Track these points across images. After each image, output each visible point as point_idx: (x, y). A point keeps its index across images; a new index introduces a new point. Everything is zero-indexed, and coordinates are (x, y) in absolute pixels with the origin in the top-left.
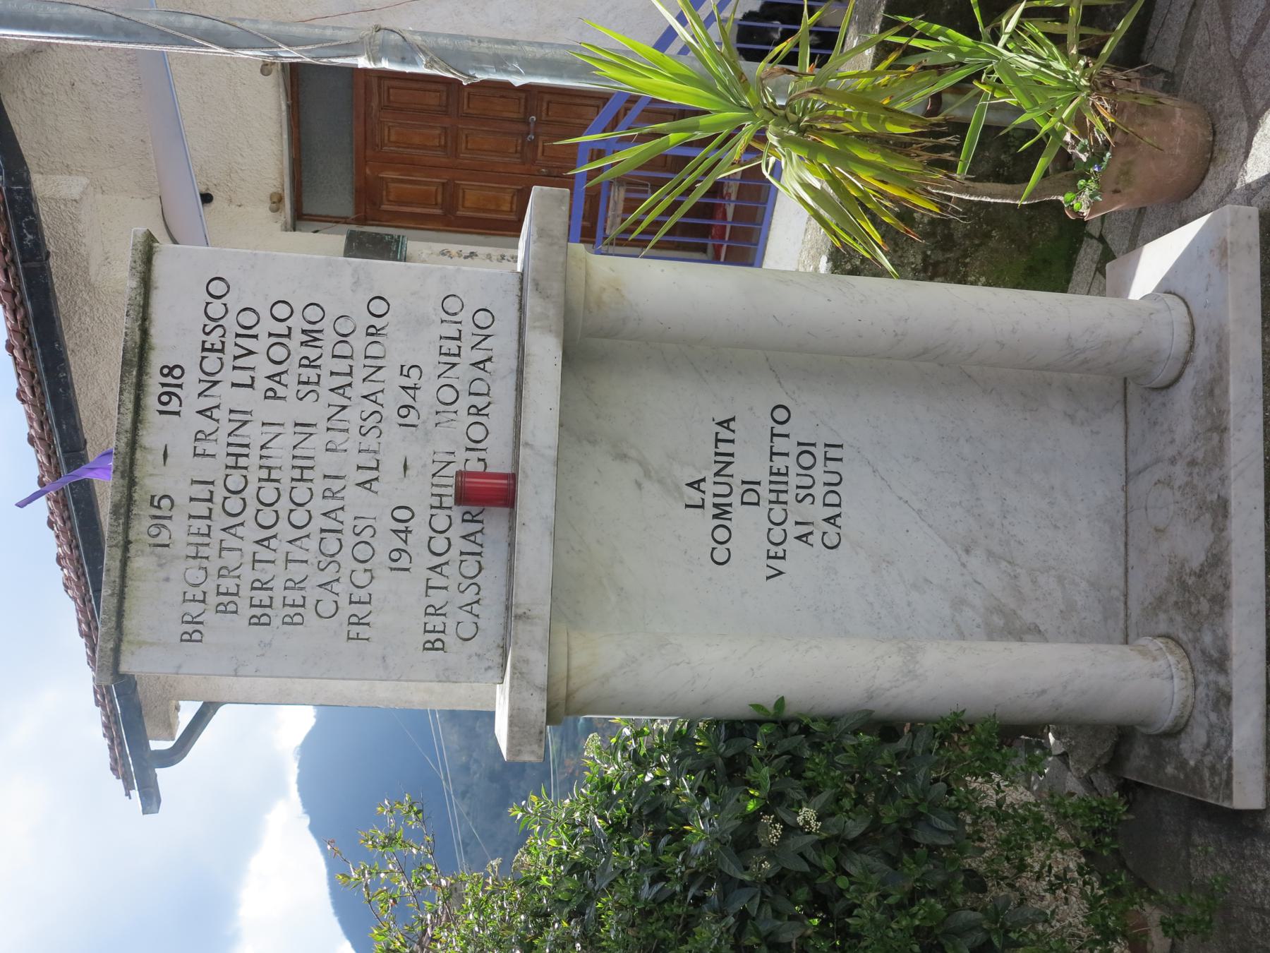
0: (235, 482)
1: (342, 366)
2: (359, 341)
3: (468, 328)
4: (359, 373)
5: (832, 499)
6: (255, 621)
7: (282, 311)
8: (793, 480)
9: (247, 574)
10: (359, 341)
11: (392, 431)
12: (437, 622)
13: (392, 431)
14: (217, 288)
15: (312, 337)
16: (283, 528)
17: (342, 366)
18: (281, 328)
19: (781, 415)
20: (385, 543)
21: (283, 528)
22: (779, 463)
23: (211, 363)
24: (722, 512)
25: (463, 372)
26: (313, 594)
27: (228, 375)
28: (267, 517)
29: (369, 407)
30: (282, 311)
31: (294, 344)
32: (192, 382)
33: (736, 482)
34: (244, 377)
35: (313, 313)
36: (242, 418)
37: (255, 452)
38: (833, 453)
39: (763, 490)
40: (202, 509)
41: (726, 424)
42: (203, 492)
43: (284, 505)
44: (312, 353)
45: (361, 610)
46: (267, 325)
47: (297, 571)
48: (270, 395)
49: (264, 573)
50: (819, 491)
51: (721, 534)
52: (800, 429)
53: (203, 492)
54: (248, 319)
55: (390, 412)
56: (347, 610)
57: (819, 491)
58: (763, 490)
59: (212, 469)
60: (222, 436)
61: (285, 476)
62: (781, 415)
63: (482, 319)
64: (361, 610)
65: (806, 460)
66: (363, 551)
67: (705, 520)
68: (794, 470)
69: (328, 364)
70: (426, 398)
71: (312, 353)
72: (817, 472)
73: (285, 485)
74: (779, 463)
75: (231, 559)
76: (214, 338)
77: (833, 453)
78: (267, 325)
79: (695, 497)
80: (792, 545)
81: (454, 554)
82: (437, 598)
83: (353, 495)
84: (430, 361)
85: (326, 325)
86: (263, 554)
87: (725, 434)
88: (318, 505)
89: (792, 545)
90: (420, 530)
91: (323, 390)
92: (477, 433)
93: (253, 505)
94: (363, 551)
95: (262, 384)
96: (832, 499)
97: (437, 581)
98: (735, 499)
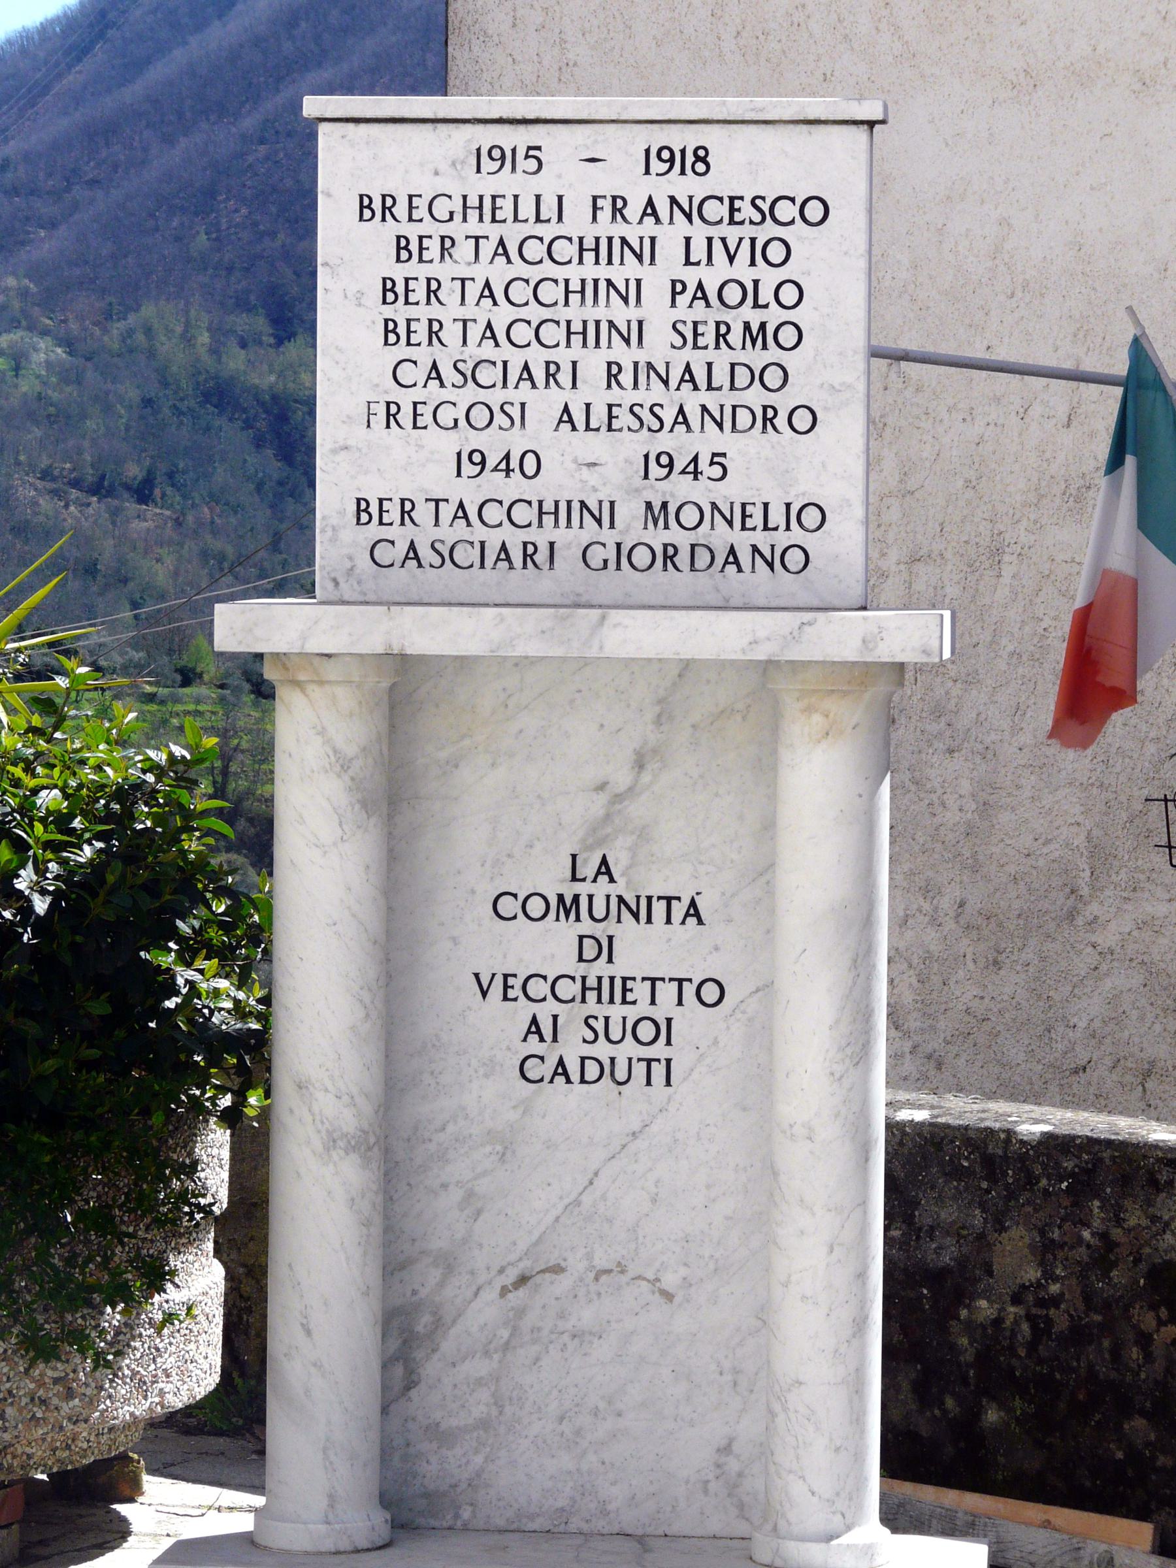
0: (564, 250)
1: (721, 376)
2: (755, 397)
3: (782, 539)
4: (711, 400)
5: (592, 1070)
6: (388, 287)
7: (789, 295)
8: (616, 1012)
9: (444, 271)
10: (755, 397)
11: (635, 445)
12: (394, 515)
13: (635, 445)
14: (814, 211)
15: (756, 335)
16: (502, 316)
17: (721, 376)
18: (766, 295)
19: (710, 993)
20: (493, 443)
21: (502, 316)
22: (641, 991)
23: (714, 210)
24: (568, 907)
25: (721, 536)
26: (424, 355)
27: (699, 233)
28: (520, 292)
29: (668, 415)
30: (789, 295)
31: (748, 313)
32: (687, 187)
33: (611, 927)
34: (699, 251)
35: (788, 336)
36: (647, 252)
37: (603, 272)
38: (658, 1070)
39: (601, 968)
40: (527, 209)
41: (693, 910)
42: (549, 209)
43: (535, 313)
44: (735, 337)
45: (406, 417)
46: (769, 278)
47: (450, 335)
48: (677, 288)
49: (449, 292)
50: (602, 1050)
51: (536, 907)
52: (691, 1021)
53: (549, 209)
54: (776, 252)
55: (665, 442)
56: (406, 399)
57: (602, 1050)
58: (601, 968)
59: (578, 222)
60: (619, 230)
61: (575, 313)
62: (710, 993)
63: (795, 559)
64: (406, 417)
65: (646, 1031)
66: (480, 416)
67: (554, 883)
68: (632, 1013)
69: (722, 359)
70: (681, 488)
71: (735, 337)
72: (629, 1048)
73: (562, 313)
74: (641, 991)
75: (465, 250)
76: (747, 211)
77: (658, 1070)
78: (769, 278)
79: (588, 868)
80: (524, 1011)
81: (479, 532)
82: (423, 513)
83: (556, 398)
84: (730, 492)
85: (774, 354)
86: (473, 290)
87: (679, 910)
88: (537, 358)
89: (524, 1011)
90: (512, 487)
91: (688, 354)
92: (642, 557)
93: (534, 273)
94: (480, 416)
95: (691, 276)
96: (592, 1070)
97: (447, 511)
98: (586, 926)
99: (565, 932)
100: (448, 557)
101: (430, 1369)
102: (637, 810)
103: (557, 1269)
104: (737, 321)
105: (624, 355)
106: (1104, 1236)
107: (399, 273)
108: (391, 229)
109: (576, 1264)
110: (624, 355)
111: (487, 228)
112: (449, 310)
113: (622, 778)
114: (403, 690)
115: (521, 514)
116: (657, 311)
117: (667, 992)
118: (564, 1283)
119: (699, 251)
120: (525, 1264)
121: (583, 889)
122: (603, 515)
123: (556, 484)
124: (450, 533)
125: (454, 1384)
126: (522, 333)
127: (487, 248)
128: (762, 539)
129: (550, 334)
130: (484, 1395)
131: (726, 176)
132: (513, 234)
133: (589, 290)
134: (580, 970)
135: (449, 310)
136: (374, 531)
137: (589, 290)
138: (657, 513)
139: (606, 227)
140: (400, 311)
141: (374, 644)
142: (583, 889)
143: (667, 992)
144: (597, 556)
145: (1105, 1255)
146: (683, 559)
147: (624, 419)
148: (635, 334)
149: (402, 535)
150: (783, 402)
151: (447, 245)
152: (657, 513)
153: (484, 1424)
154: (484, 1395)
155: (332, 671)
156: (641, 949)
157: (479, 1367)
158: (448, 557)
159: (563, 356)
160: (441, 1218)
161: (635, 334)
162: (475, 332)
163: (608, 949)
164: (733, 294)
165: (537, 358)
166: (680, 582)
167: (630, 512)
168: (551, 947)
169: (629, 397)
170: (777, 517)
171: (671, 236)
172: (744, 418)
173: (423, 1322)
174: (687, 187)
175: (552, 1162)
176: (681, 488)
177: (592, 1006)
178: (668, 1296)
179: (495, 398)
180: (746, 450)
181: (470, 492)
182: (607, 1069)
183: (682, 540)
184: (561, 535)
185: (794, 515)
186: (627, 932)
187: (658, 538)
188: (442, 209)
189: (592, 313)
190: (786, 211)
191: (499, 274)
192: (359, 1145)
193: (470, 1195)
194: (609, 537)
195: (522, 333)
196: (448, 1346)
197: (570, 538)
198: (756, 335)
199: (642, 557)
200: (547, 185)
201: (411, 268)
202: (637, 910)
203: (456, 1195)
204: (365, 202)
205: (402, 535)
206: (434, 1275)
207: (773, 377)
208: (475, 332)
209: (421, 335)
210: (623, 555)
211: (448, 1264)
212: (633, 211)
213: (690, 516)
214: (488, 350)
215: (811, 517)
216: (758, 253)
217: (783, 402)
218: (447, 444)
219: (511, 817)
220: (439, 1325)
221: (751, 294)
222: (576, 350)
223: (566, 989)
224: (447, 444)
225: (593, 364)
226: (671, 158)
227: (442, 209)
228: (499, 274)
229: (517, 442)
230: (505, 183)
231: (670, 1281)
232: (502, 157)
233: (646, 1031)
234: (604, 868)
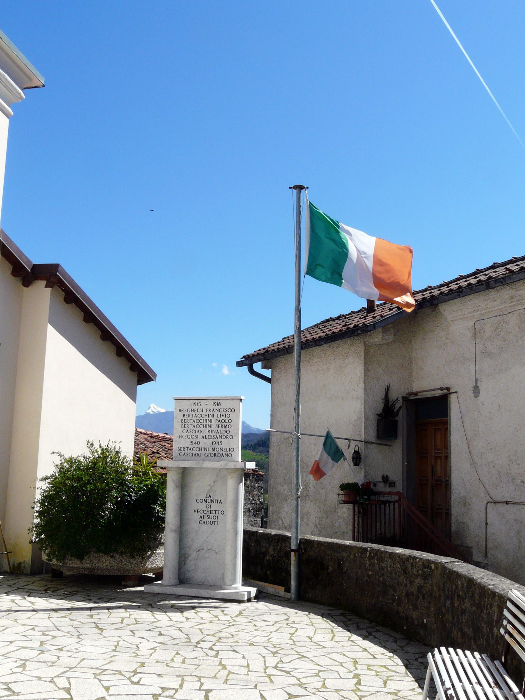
0: (203, 416)
1: (222, 432)
2: (226, 434)
3: (229, 453)
4: (220, 435)
5: (208, 523)
6: (182, 420)
7: (230, 421)
8: (211, 515)
9: (189, 418)
10: (226, 434)
11: (211, 440)
12: (182, 449)
13: (211, 440)
14: (233, 410)
15: (226, 426)
16: (196, 424)
17: (222, 432)
18: (227, 421)
19: (223, 513)
20: (194, 440)
21: (196, 424)
22: (214, 512)
23: (221, 410)
24: (205, 501)
25: (221, 452)
26: (186, 429)
27: (219, 413)
28: (198, 421)
29: (215, 437)
30: (230, 421)
31: (225, 423)
32: (218, 407)
33: (210, 504)
34: (219, 416)
35: (230, 426)
36: (213, 416)
37: (208, 418)
38: (216, 523)
39: (209, 509)
40: (199, 411)
41: (221, 502)
42: (201, 411)
43: (199, 424)
44: (223, 427)
45: (184, 437)
46: (228, 419)
47: (189, 426)
48: (216, 420)
49: (189, 421)
50: (209, 520)
51: (201, 501)
52: (220, 516)
53: (201, 411)
54: (228, 416)
55: (215, 440)
56: (184, 435)
57: (209, 520)
58: (209, 509)
59: (205, 412)
60: (210, 413)
61: (204, 424)
62: (223, 513)
63: (230, 455)
64: (184, 437)
65: (215, 517)
66: (193, 437)
67: (204, 498)
68: (213, 515)
69: (222, 429)
70: (217, 446)
71: (223, 427)
72: (212, 520)
73: (203, 424)
74: (214, 512)
75: (191, 416)
76: (225, 410)
77: (216, 523)
78: (228, 419)
79: (208, 496)
80: (200, 514)
81: (192, 452)
82: (186, 449)
83: (202, 434)
84: (223, 446)
85: (228, 429)
86: (192, 421)
87: (219, 501)
88: (200, 429)
89: (200, 514)
90: (196, 446)
91: (218, 429)
92: (212, 455)
93: (199, 419)
94: (193, 437)
95: (218, 419)
96: (208, 523)
97: (189, 449)
98: (207, 504)
99: (205, 504)
100: (188, 455)
101: (187, 562)
102: (214, 488)
103: (203, 549)
104: (223, 424)
105: (210, 429)
106: (280, 548)
107: (183, 419)
108: (183, 413)
109: (205, 549)
110: (210, 429)
111: (194, 413)
112: (189, 424)
113: (212, 484)
114: (184, 472)
115: (197, 449)
116: (214, 423)
117: (217, 512)
118: (204, 551)
119: (219, 416)
120: (199, 548)
121: (207, 499)
122: (207, 449)
123: (202, 445)
124: (189, 452)
125: (190, 564)
126: (198, 426)
127: (194, 415)
128: (226, 453)
129: (201, 426)
130: (194, 566)
131: (222, 406)
132: (197, 414)
133: (206, 421)
134: (206, 509)
135: (189, 424)
136: (180, 452)
137: (206, 421)
138: (214, 449)
139: (208, 413)
140: (183, 424)
141: (176, 466)
142: (207, 499)
143: (217, 512)
144: (206, 455)
145: (280, 551)
146: (217, 455)
147: (210, 437)
148: (211, 426)
149: (183, 452)
150: (229, 435)
151: (189, 415)
152: (214, 449)
153: (194, 570)
154: (194, 566)
155: (172, 469)
156: (214, 507)
157: (193, 562)
158: (188, 455)
159: (203, 429)
160: (189, 541)
161: (211, 426)
162: (192, 426)
163: (210, 506)
164: (223, 421)
165: (200, 429)
166: (216, 458)
167: (210, 449)
168: (203, 506)
169: (211, 434)
170: (228, 450)
171: (216, 414)
172: (224, 437)
173: (187, 556)
174: (218, 407)
175: (200, 535)
176: (217, 446)
177: (208, 514)
178: (217, 553)
179: (194, 434)
180: (224, 441)
181: (191, 446)
182: (210, 522)
183: (216, 453)
184: (202, 452)
185: (230, 449)
186: (212, 504)
187: (214, 452)
188: (189, 411)
189: (206, 424)
190: (230, 410)
191: (195, 419)
192: (175, 531)
193: (193, 539)
194: (208, 452)
195: (198, 426)
196: (190, 558)
197: (203, 452)
198: (226, 426)
199: (212, 455)
200: (201, 407)
201: (185, 418)
202: (213, 501)
203: (191, 539)
204: (180, 410)
205: (183, 452)
206: (188, 550)
207: (228, 432)
208: (192, 426)
209: (186, 426)
210: (209, 454)
211: (190, 548)
212: (211, 411)
213: (218, 450)
214: (194, 429)
215: (232, 450)
216: (226, 416)
217: (229, 435)
218: (189, 440)
219: (198, 488)
220: (189, 556)
221: (225, 421)
222: (204, 428)
223: (205, 512)
224: (189, 440)
225: (206, 430)
226: (216, 404)
227: (189, 411)
228: (195, 419)
229: (197, 440)
230: (196, 407)
231: (217, 551)
232: (196, 404)
233: (215, 517)
234: (210, 496)
